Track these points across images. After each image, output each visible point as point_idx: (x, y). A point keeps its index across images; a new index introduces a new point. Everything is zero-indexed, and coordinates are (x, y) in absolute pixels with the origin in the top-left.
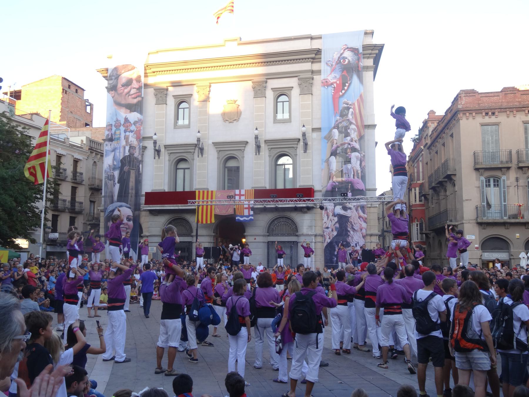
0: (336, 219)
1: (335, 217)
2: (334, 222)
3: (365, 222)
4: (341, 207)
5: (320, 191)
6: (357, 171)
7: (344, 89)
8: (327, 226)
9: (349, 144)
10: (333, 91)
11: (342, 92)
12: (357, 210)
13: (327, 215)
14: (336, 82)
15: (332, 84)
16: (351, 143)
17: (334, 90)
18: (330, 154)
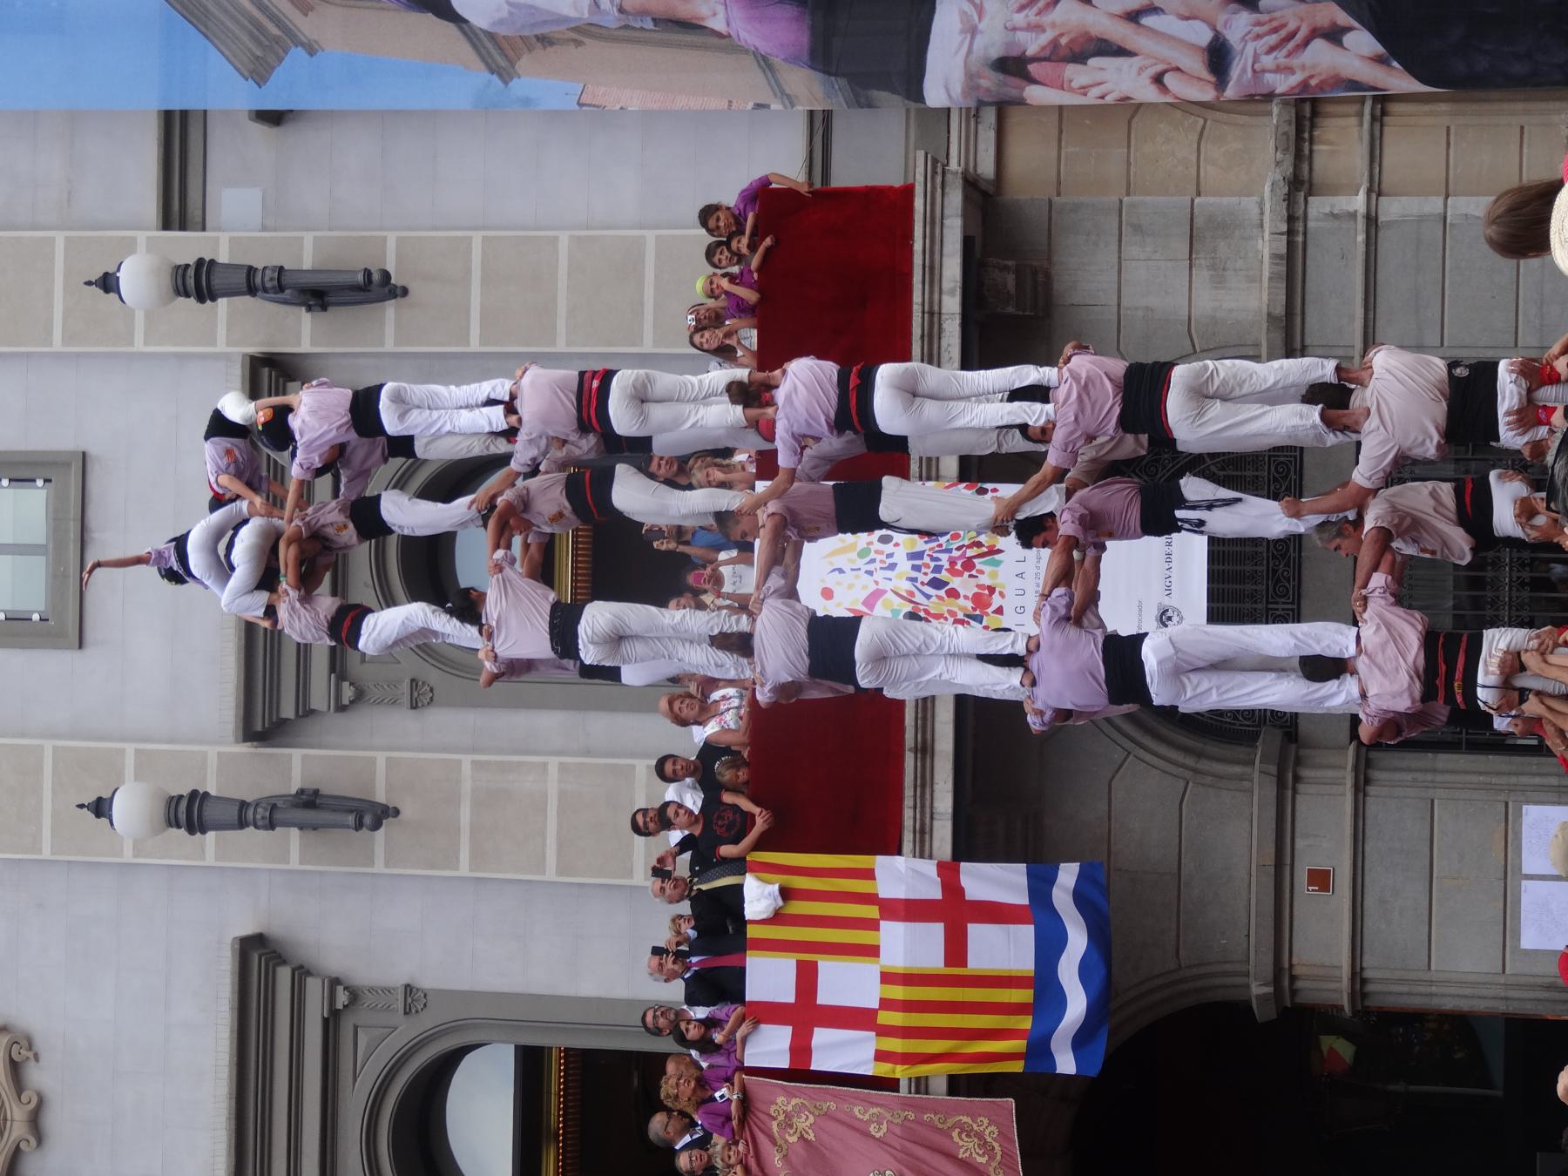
5: (821, 127)
8: (1196, 65)
18: (430, 17)
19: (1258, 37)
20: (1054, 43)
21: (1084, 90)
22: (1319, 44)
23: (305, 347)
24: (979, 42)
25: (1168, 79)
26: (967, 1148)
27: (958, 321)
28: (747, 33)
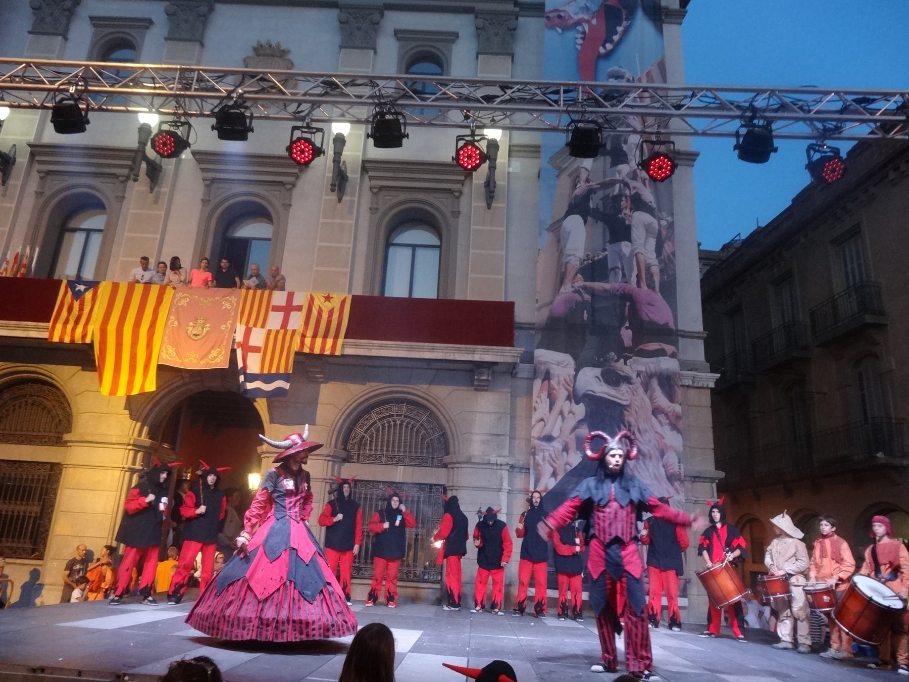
0: (580, 410)
1: (577, 403)
2: (571, 422)
3: (674, 427)
4: (598, 371)
6: (648, 268)
7: (611, 41)
8: (546, 432)
9: (626, 185)
10: (580, 41)
11: (605, 48)
12: (647, 387)
13: (550, 396)
14: (588, 22)
15: (579, 23)
16: (632, 183)
17: (583, 39)
18: (566, 209)
19: (554, 451)
20: (554, 389)
21: (539, 397)
22: (551, 470)
23: (474, 181)
24: (555, 366)
25: (542, 423)
26: (214, 353)
27: (472, 359)
28: (559, 298)
